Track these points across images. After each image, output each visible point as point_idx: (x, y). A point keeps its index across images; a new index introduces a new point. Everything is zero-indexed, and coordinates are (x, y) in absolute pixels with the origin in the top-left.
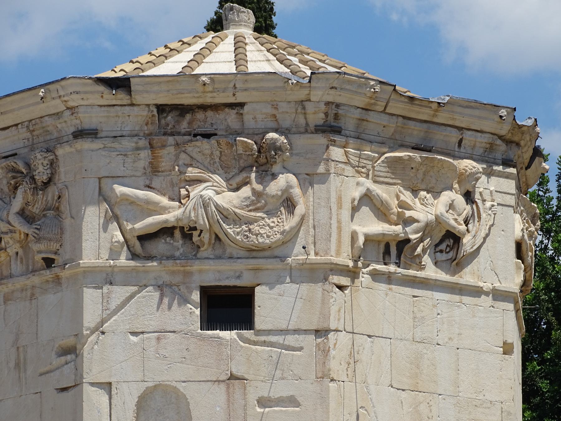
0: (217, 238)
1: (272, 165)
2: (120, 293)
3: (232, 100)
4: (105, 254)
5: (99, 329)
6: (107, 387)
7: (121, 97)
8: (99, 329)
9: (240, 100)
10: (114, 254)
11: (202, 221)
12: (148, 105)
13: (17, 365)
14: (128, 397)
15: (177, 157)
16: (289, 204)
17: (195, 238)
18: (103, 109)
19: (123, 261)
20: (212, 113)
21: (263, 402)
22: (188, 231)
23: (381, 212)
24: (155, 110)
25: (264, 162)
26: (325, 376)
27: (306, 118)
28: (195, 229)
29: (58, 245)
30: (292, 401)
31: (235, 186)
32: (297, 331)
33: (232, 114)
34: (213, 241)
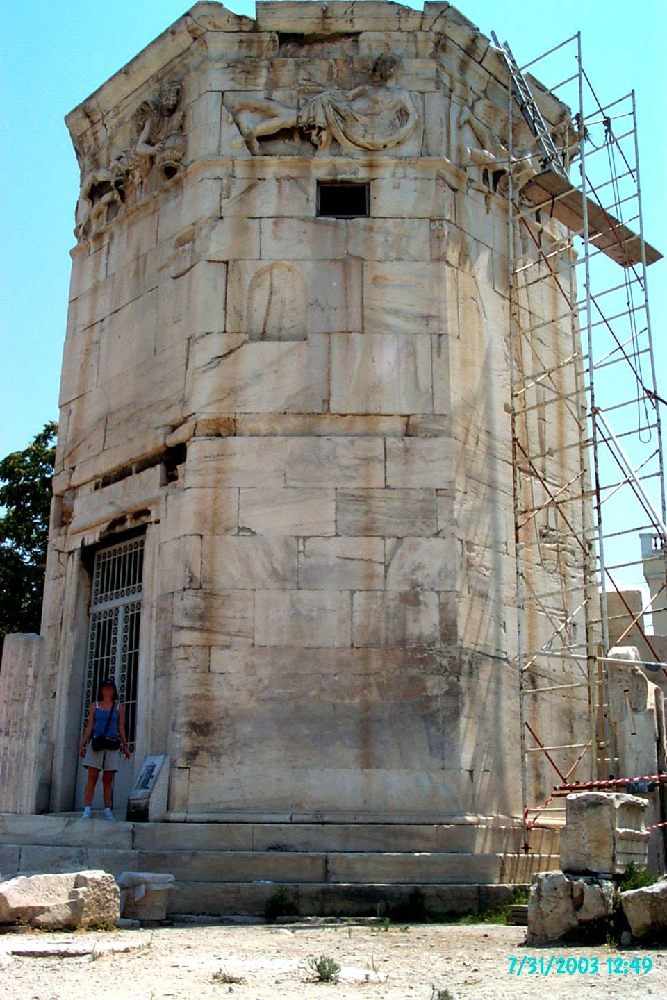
0: (335, 140)
1: (386, 80)
3: (347, 28)
9: (357, 28)
12: (271, 32)
13: (137, 273)
15: (296, 74)
18: (228, 34)
20: (329, 44)
22: (306, 130)
24: (277, 36)
27: (416, 47)
28: (313, 127)
29: (181, 154)
31: (351, 98)
33: (348, 42)
34: (329, 143)
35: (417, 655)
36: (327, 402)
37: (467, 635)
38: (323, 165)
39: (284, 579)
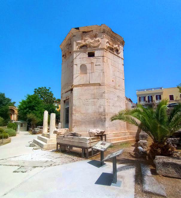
2: (78, 54)
3: (91, 30)
4: (76, 49)
5: (76, 58)
6: (76, 65)
7: (77, 31)
8: (76, 58)
10: (77, 49)
11: (88, 43)
14: (79, 66)
16: (99, 41)
17: (87, 47)
19: (78, 50)
21: (96, 65)
23: (110, 44)
25: (96, 36)
26: (103, 62)
30: (99, 65)
32: (100, 57)
35: (101, 114)
36: (89, 82)
37: (106, 111)
38: (89, 50)
39: (85, 105)
